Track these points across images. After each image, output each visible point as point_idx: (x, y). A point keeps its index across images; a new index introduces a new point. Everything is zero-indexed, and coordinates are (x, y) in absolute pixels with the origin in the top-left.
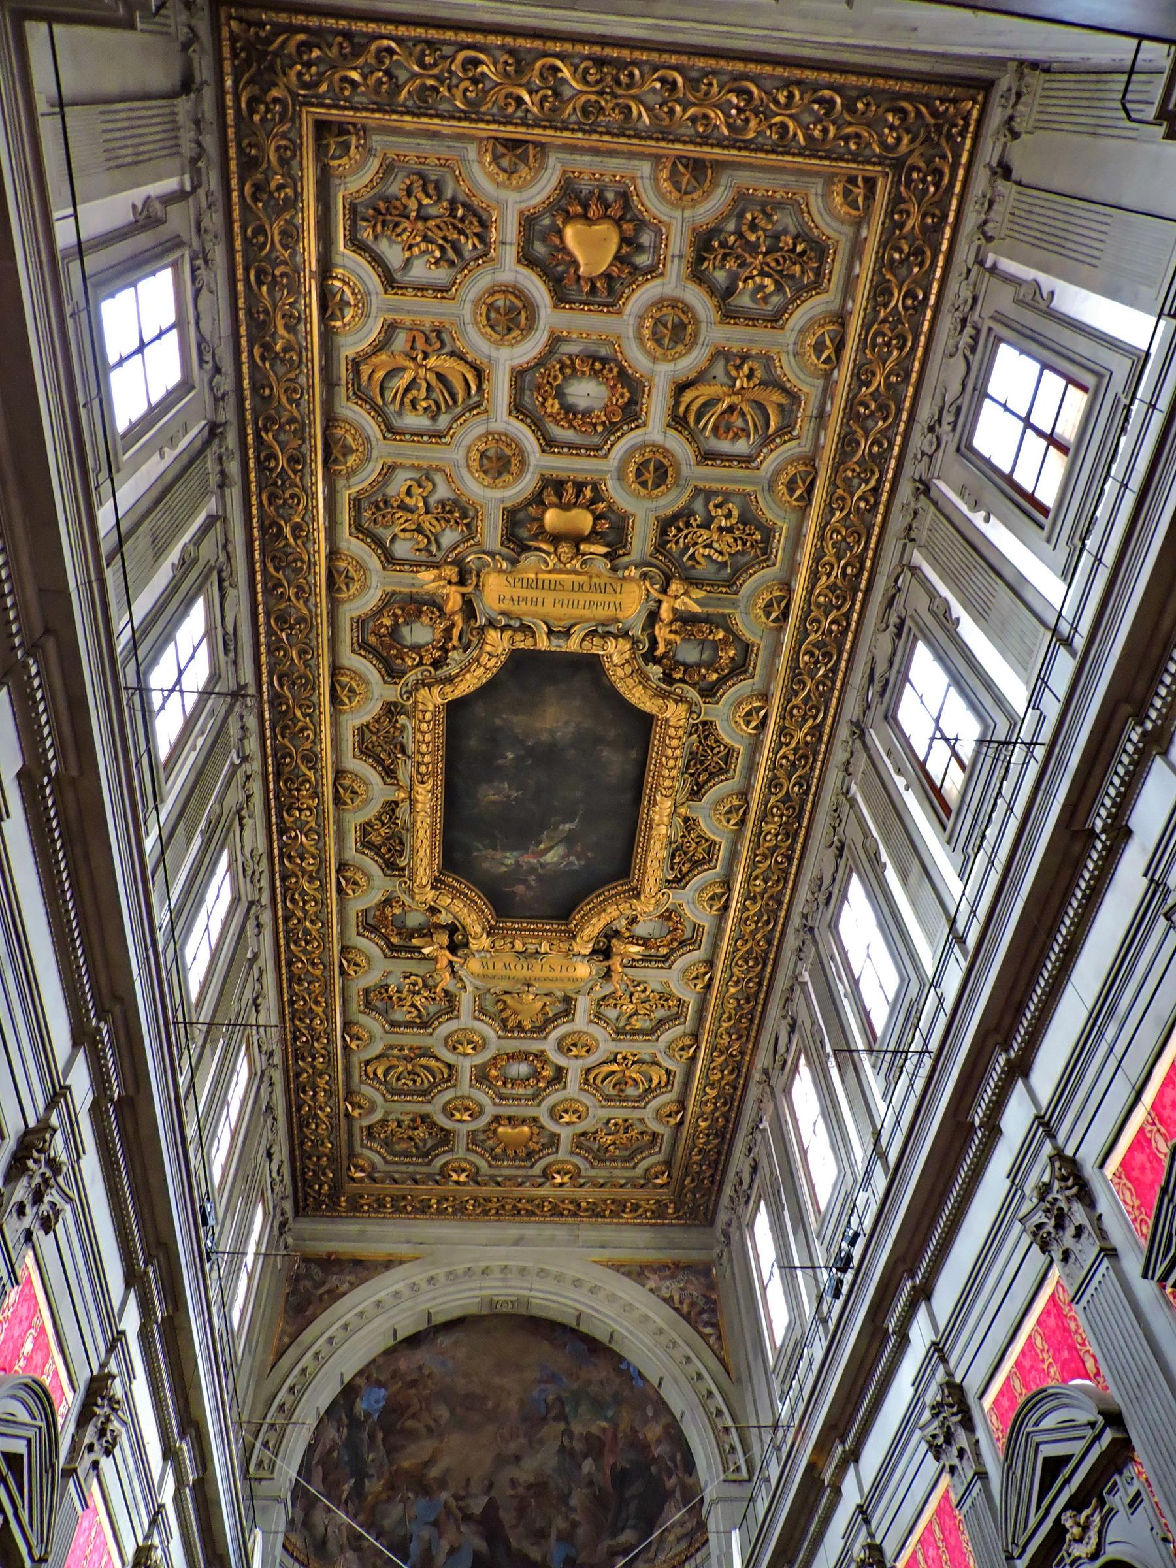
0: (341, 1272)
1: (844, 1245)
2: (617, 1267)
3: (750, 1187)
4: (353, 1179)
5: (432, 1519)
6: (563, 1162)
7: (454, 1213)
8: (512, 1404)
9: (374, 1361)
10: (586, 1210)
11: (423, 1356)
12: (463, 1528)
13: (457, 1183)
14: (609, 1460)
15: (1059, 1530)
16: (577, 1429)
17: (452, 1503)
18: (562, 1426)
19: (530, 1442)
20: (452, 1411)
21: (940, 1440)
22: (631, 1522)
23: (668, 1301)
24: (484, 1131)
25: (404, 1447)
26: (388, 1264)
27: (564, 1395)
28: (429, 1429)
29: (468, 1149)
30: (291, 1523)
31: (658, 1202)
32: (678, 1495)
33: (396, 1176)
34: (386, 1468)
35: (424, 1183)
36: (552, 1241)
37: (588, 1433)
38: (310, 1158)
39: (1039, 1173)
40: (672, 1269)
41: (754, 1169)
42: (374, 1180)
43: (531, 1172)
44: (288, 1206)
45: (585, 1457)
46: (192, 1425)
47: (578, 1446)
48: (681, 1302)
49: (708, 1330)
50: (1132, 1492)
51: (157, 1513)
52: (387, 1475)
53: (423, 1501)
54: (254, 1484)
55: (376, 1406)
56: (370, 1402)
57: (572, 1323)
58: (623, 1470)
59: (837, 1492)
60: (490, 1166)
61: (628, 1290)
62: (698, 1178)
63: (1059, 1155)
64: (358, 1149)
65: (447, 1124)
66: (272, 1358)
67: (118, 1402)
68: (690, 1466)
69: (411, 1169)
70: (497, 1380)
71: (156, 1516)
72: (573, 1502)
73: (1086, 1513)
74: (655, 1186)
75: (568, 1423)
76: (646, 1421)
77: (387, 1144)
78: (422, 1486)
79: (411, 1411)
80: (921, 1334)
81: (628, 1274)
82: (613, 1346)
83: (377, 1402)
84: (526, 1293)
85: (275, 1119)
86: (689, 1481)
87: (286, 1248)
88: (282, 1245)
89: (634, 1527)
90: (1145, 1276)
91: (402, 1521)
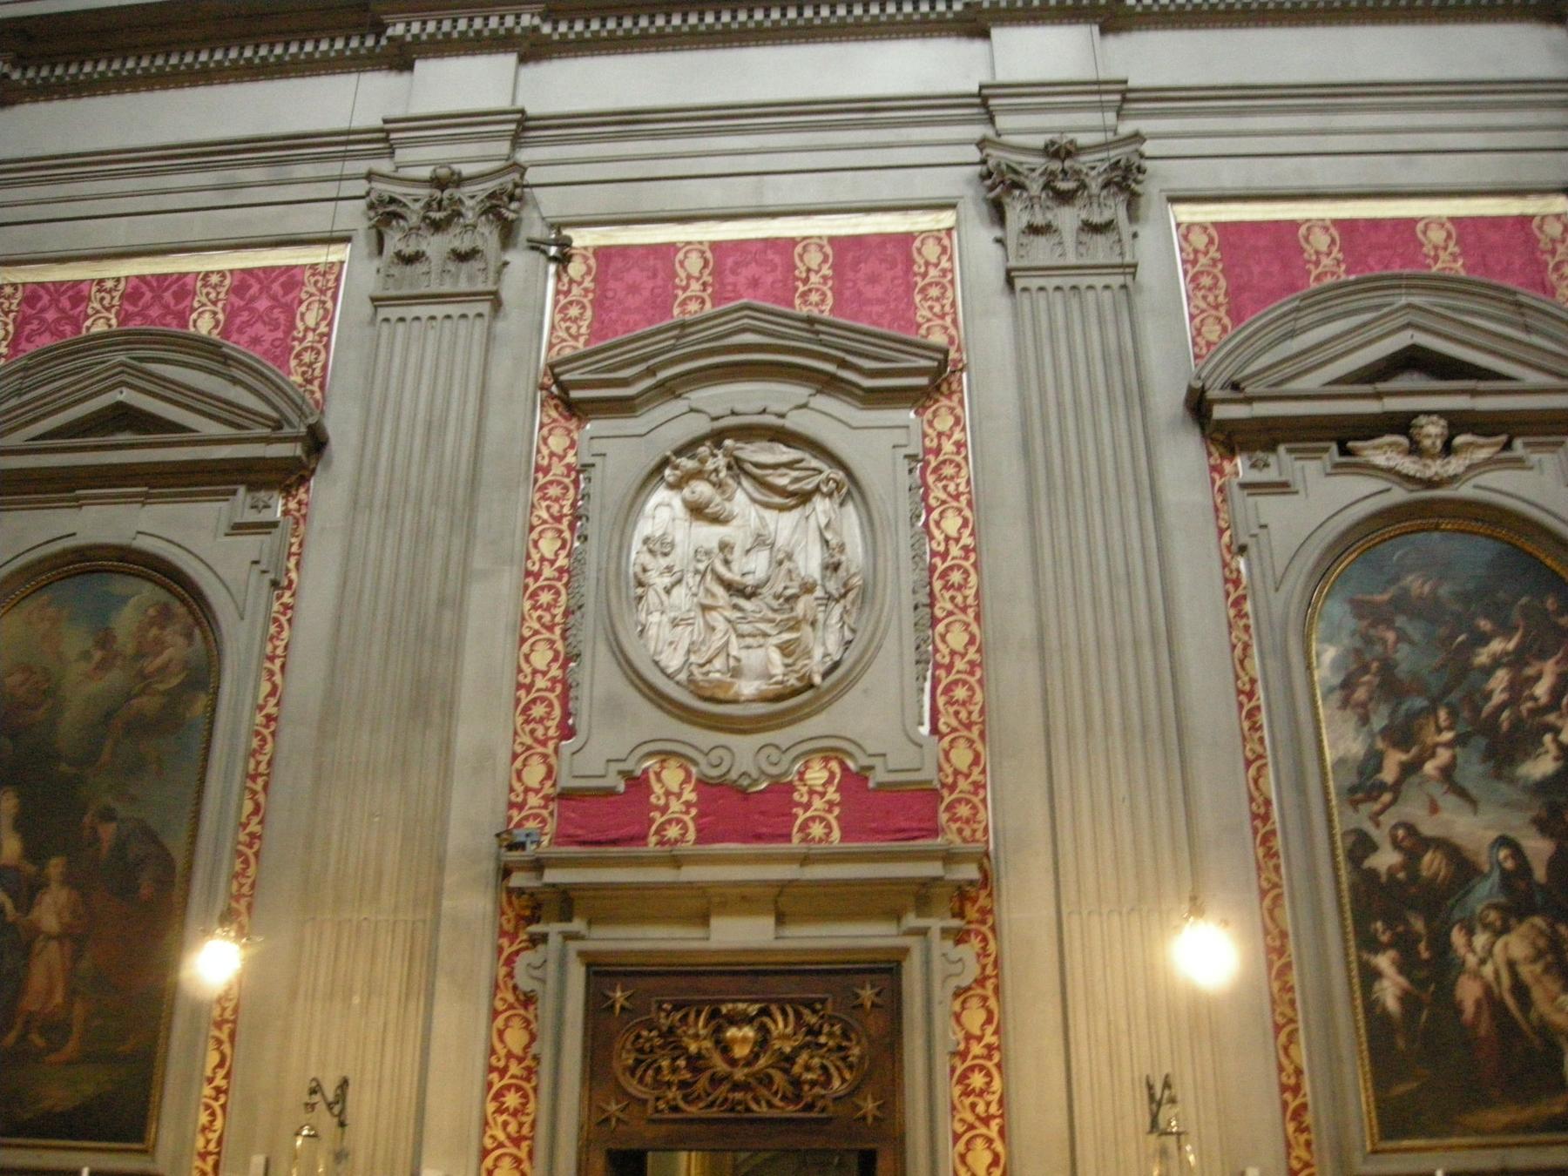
15: (1402, 424)
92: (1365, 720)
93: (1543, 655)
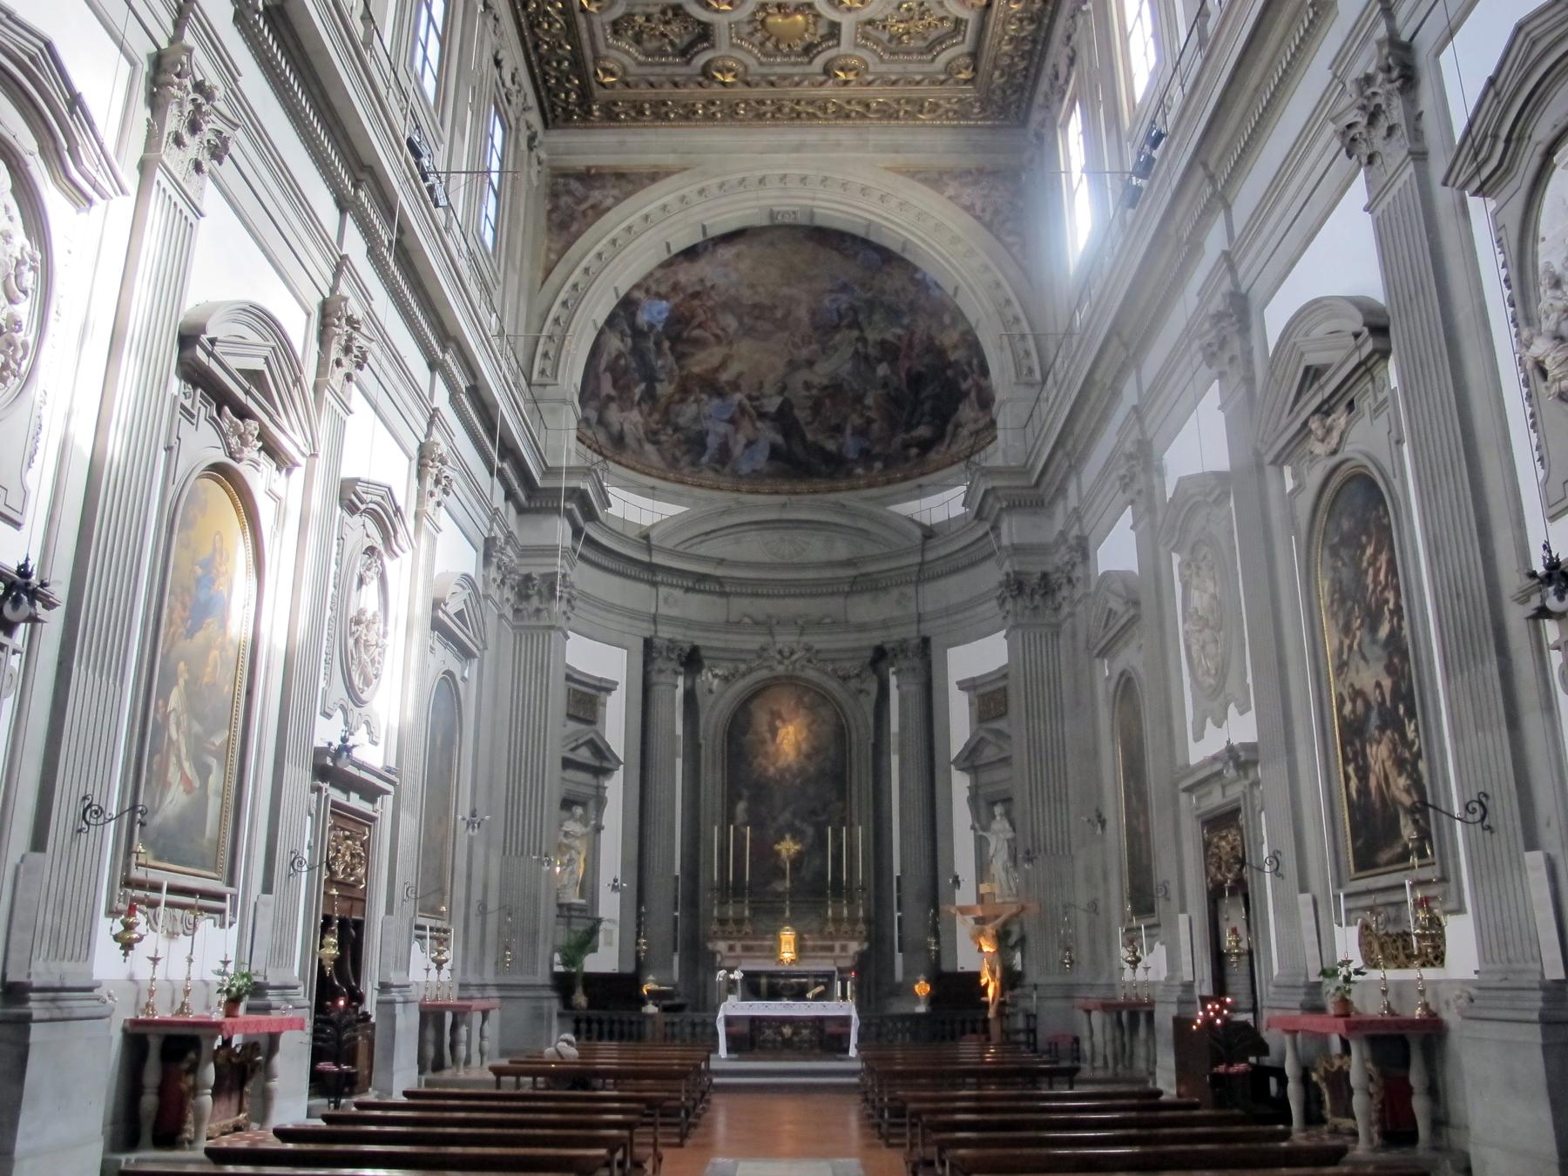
0: (603, 187)
1: (1147, 147)
2: (913, 173)
3: (1067, 81)
4: (603, 85)
5: (726, 417)
6: (846, 56)
7: (723, 119)
8: (802, 313)
9: (651, 274)
10: (877, 111)
11: (704, 270)
12: (759, 424)
13: (724, 84)
14: (904, 364)
16: (872, 336)
18: (855, 333)
20: (741, 323)
21: (1215, 348)
22: (927, 419)
23: (968, 209)
24: (750, 22)
25: (693, 354)
26: (655, 176)
27: (857, 304)
28: (717, 336)
29: (733, 45)
30: (584, 421)
31: (960, 100)
32: (973, 395)
33: (652, 79)
34: (677, 372)
35: (685, 86)
36: (838, 145)
38: (549, 63)
39: (1367, 61)
40: (977, 175)
41: (1072, 61)
42: (627, 85)
43: (809, 69)
44: (534, 117)
45: (880, 361)
46: (448, 336)
47: (872, 351)
48: (983, 210)
49: (1010, 239)
50: (1381, 397)
51: (432, 417)
52: (677, 379)
53: (716, 401)
54: (537, 391)
56: (653, 313)
57: (861, 232)
58: (920, 374)
59: (1115, 392)
60: (761, 64)
61: (924, 198)
62: (1009, 73)
63: (1393, 40)
64: (603, 50)
65: (704, 16)
66: (540, 275)
67: (358, 322)
68: (984, 371)
69: (669, 70)
70: (786, 291)
71: (433, 417)
72: (869, 401)
73: (1333, 416)
74: (957, 82)
75: (861, 330)
76: (943, 328)
77: (637, 39)
78: (711, 385)
79: (696, 322)
80: (1215, 241)
81: (925, 181)
82: (907, 256)
83: (660, 313)
84: (809, 202)
85: (496, 19)
86: (983, 382)
87: (540, 163)
88: (534, 161)
89: (929, 423)
90: (1445, 184)
91: (696, 419)
92: (1337, 624)
93: (1381, 553)
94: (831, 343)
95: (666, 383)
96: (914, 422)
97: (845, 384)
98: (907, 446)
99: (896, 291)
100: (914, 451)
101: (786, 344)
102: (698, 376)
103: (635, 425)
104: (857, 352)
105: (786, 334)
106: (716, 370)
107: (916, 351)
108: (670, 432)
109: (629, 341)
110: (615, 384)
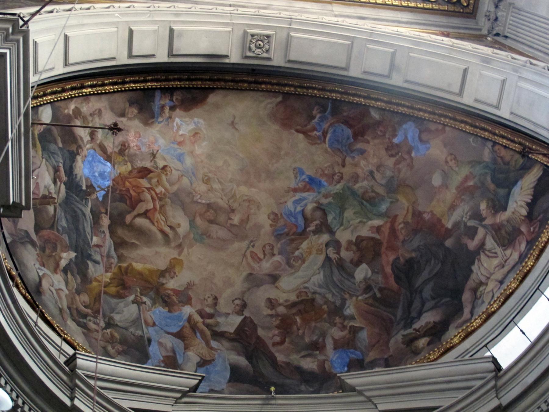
5: (175, 330)
12: (214, 344)
17: (197, 318)
18: (325, 237)
19: (288, 263)
20: (192, 222)
22: (429, 305)
25: (133, 246)
27: (324, 201)
34: (115, 260)
37: (358, 237)
45: (357, 264)
52: (114, 269)
55: (100, 182)
58: (410, 262)
70: (244, 190)
72: (350, 310)
75: (332, 232)
79: (141, 208)
91: (136, 322)
94: (297, 253)
95: (101, 268)
96: (414, 314)
97: (319, 300)
98: (410, 341)
99: (371, 173)
100: (422, 342)
101: (244, 255)
102: (140, 274)
103: (58, 290)
104: (328, 259)
105: (245, 244)
106: (162, 273)
107: (401, 237)
108: (102, 324)
109: (63, 187)
110: (38, 228)
